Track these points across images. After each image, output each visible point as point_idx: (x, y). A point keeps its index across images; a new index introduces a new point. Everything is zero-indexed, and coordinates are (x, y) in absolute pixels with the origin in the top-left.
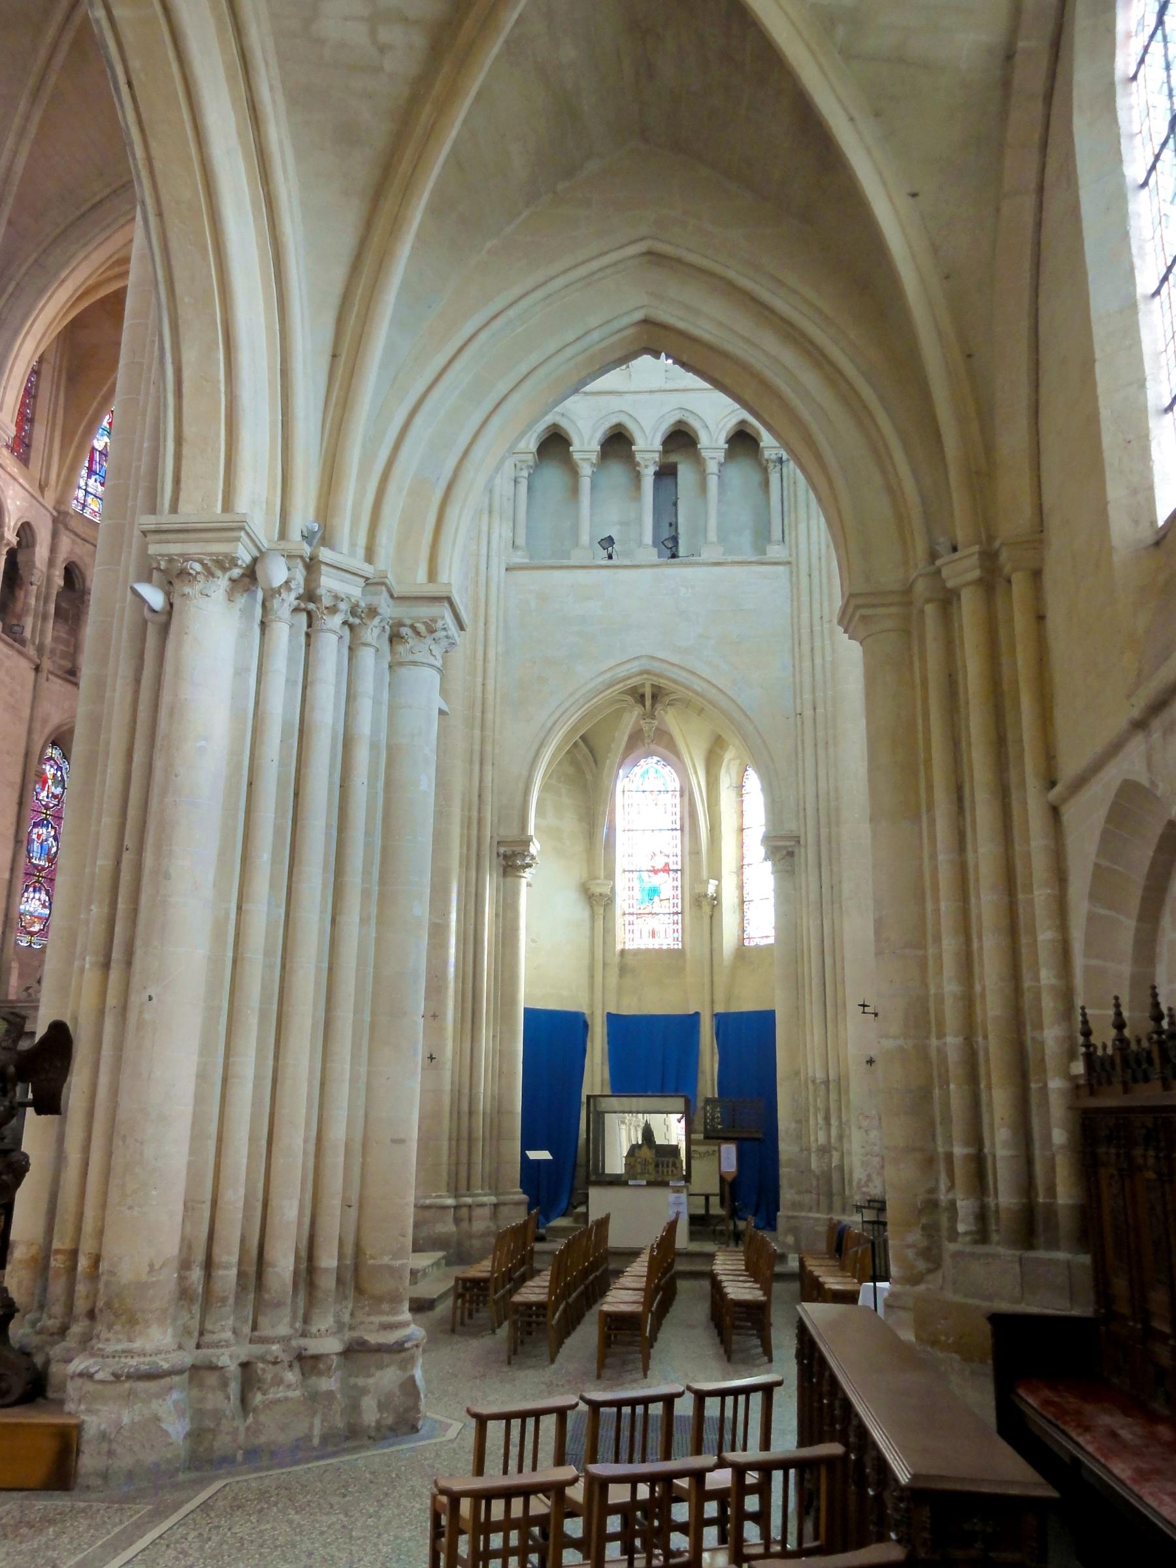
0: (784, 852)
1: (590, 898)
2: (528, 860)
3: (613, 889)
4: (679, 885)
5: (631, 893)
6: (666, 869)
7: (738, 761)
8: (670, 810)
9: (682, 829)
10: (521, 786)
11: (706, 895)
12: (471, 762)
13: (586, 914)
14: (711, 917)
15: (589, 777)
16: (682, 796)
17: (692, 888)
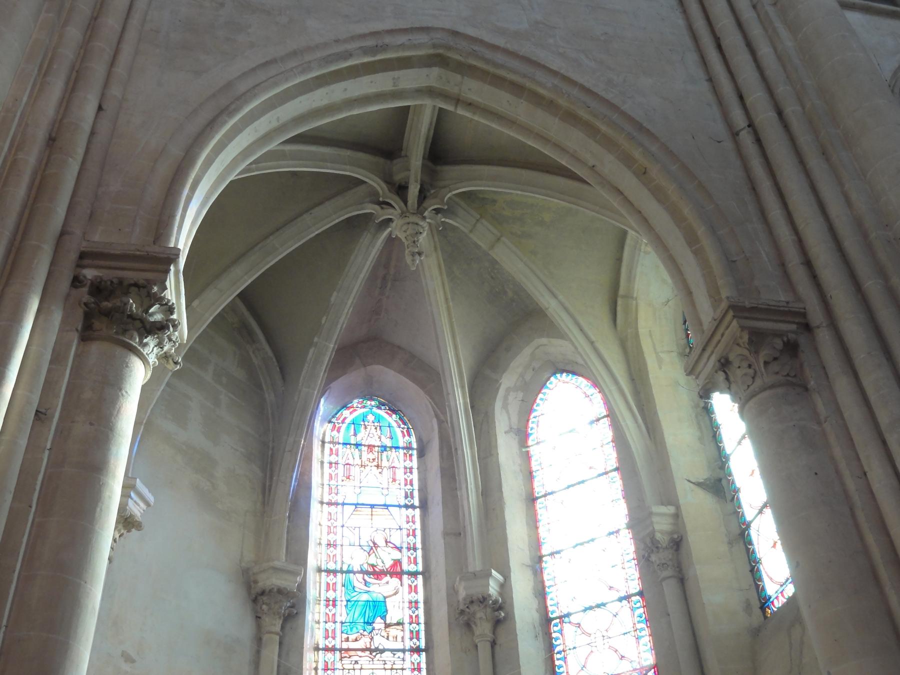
0: (779, 343)
1: (255, 601)
2: (156, 314)
3: (302, 587)
4: (420, 597)
5: (332, 610)
6: (396, 571)
7: (520, 395)
8: (400, 475)
9: (424, 506)
10: (164, 170)
11: (483, 600)
12: (45, 72)
13: (245, 630)
14: (493, 644)
15: (270, 397)
16: (421, 454)
17: (452, 591)
